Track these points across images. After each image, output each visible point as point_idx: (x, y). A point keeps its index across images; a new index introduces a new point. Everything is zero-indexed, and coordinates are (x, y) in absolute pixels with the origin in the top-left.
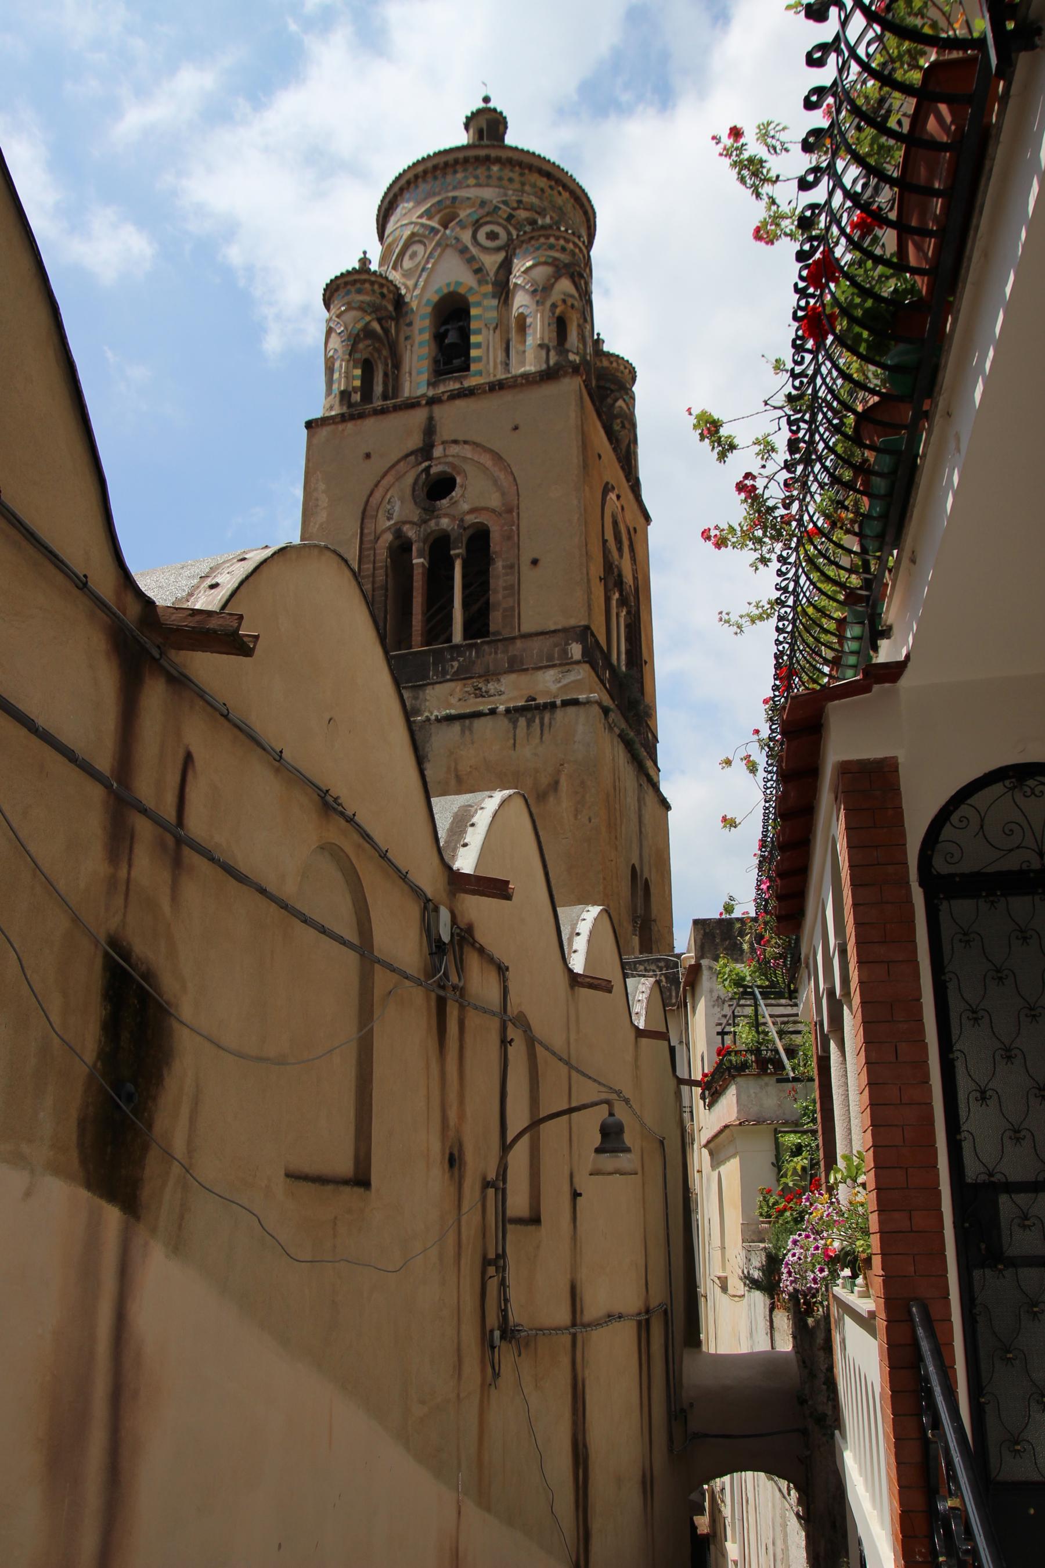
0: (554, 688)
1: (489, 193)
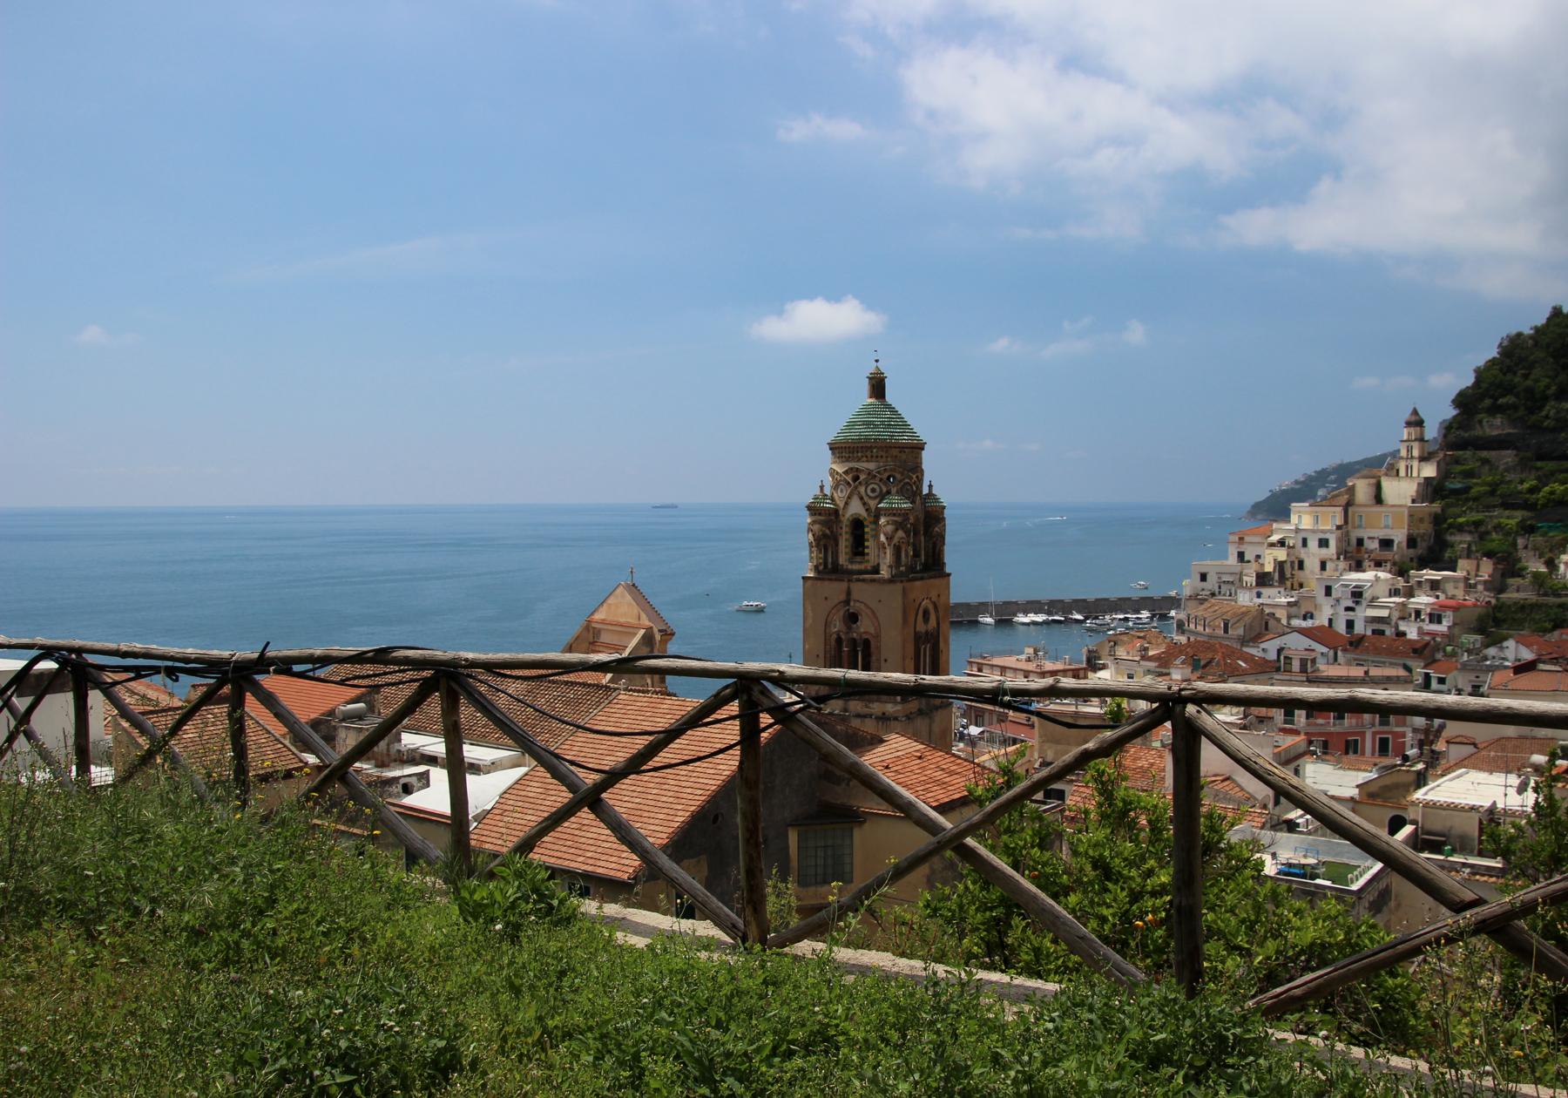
1: (872, 466)
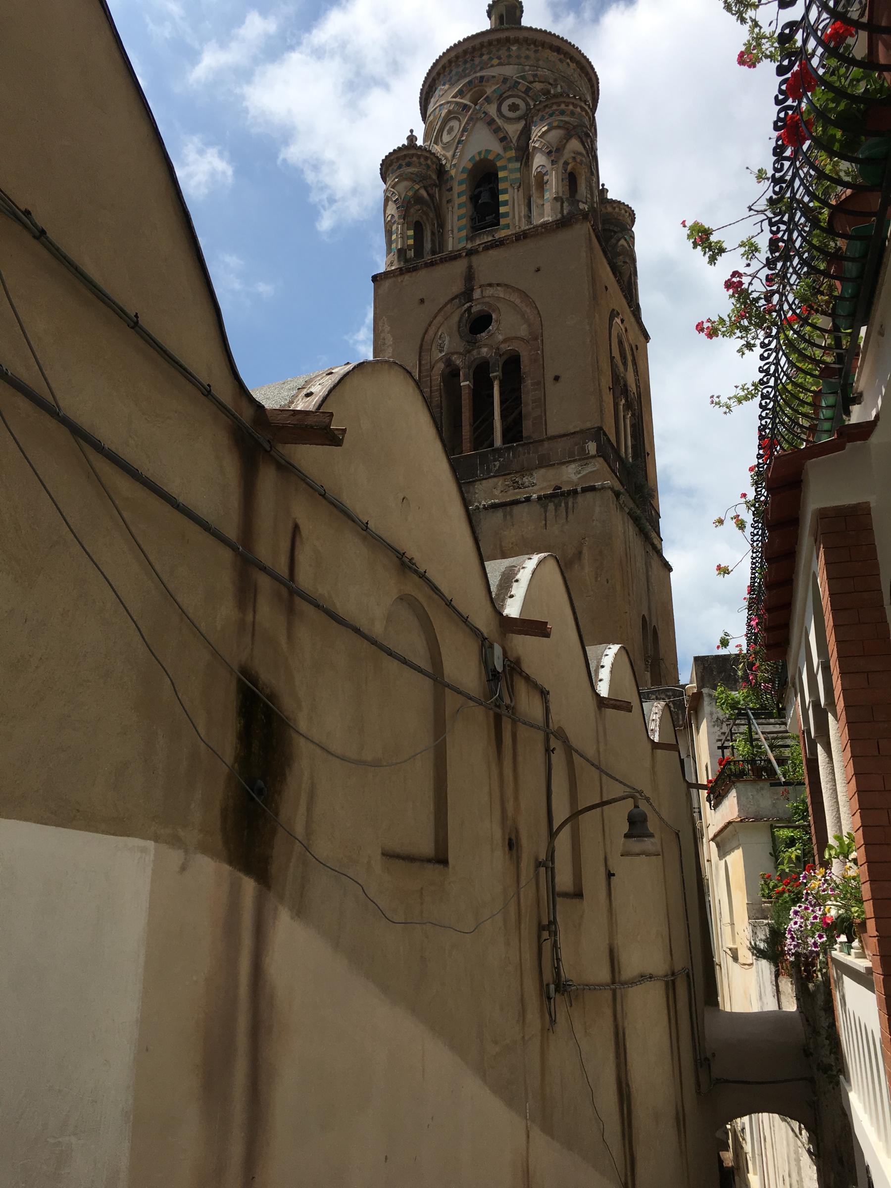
0: (575, 478)
1: (509, 71)
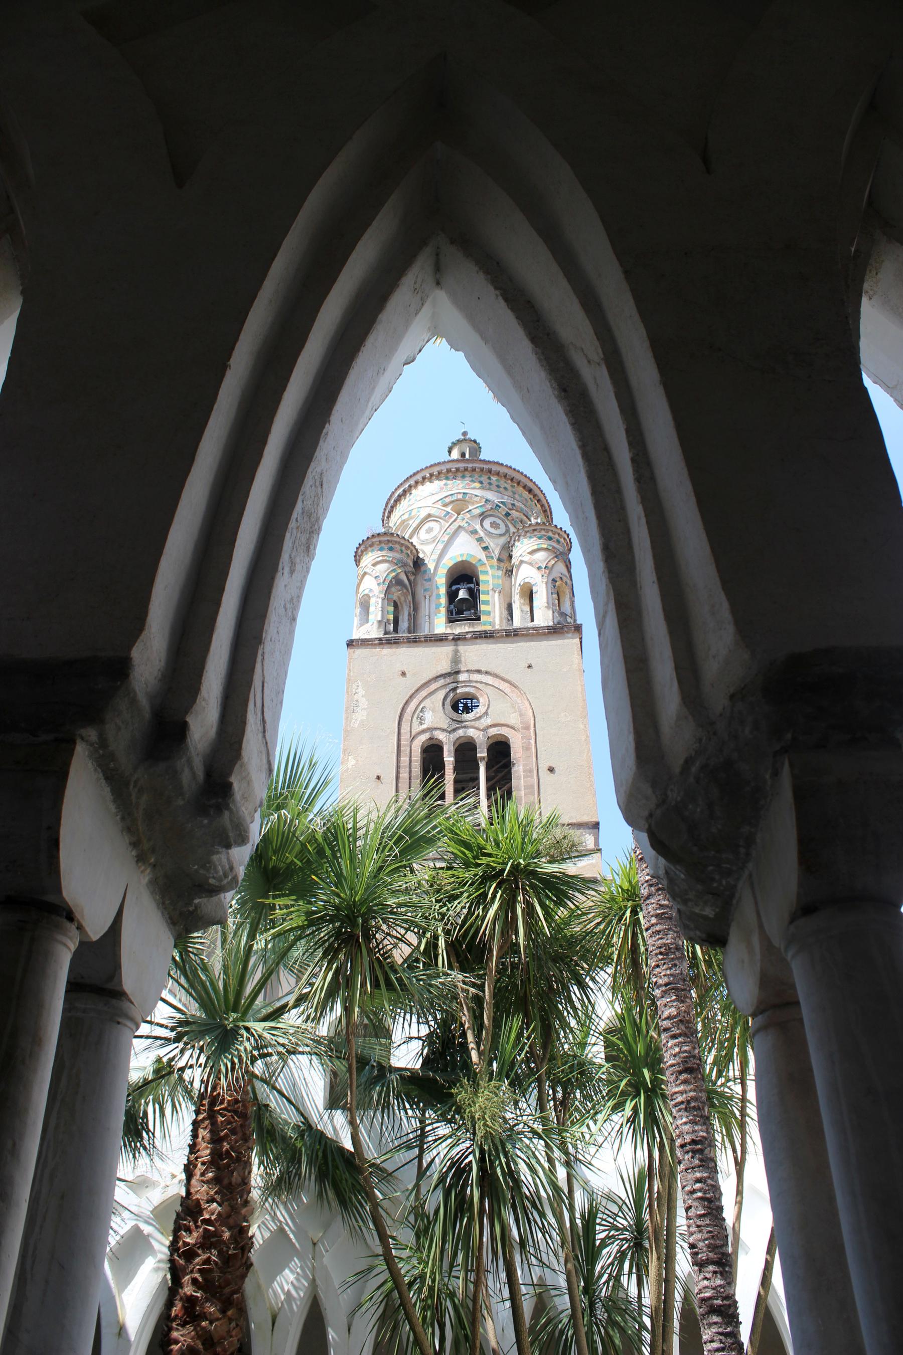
1: (490, 495)
